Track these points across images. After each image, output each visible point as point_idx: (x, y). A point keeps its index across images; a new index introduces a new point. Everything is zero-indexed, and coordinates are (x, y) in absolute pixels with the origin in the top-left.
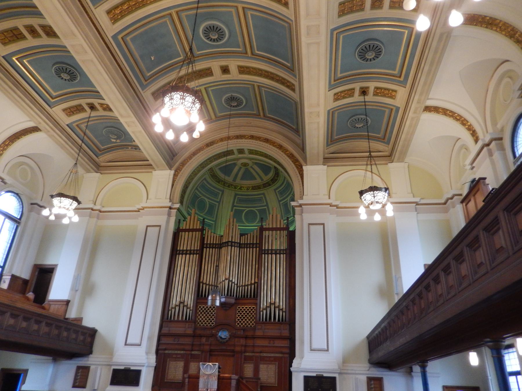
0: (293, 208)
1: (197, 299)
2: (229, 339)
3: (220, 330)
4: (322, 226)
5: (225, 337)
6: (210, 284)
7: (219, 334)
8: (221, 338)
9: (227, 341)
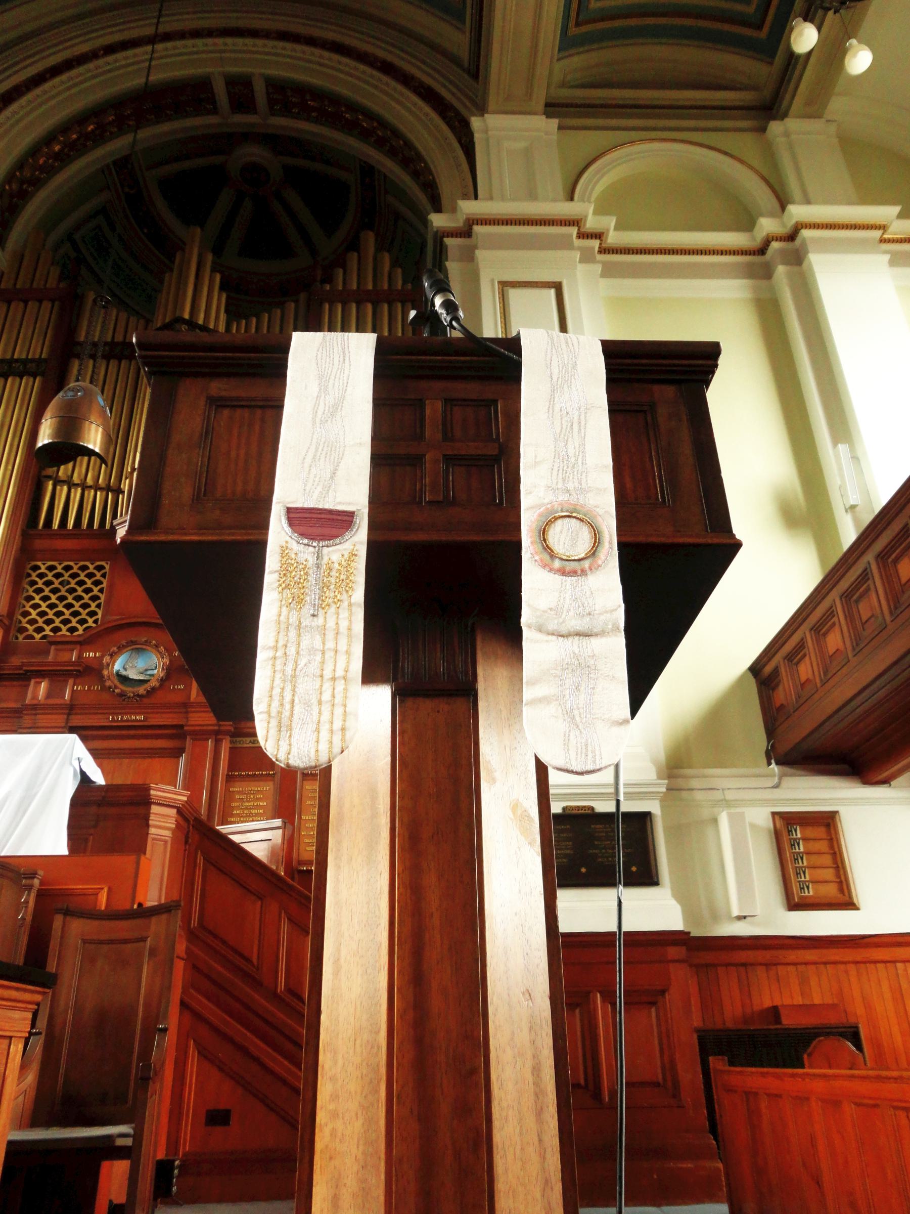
0: (441, 236)
1: (25, 535)
2: (162, 681)
3: (121, 649)
4: (552, 292)
5: (141, 677)
6: (90, 481)
7: (117, 666)
8: (124, 679)
9: (151, 692)
